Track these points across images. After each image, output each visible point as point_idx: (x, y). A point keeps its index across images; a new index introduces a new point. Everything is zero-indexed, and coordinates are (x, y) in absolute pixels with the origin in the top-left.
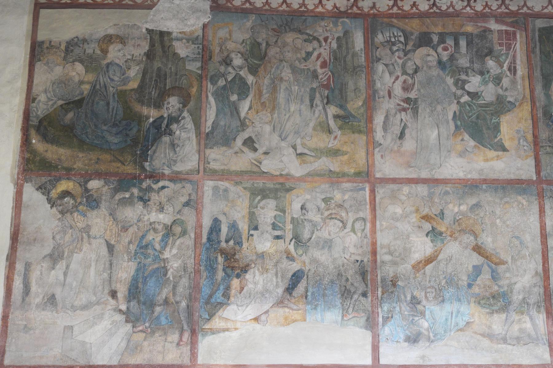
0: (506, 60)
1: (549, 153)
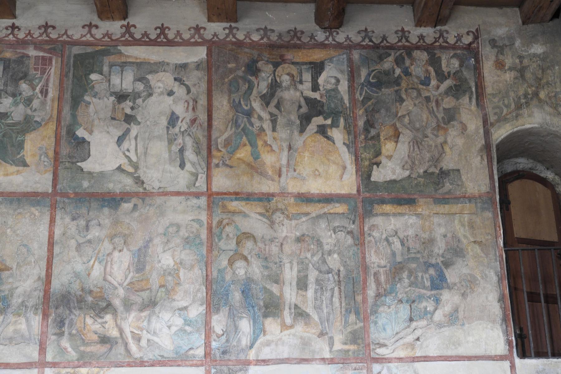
0: (39, 83)
1: (68, 168)
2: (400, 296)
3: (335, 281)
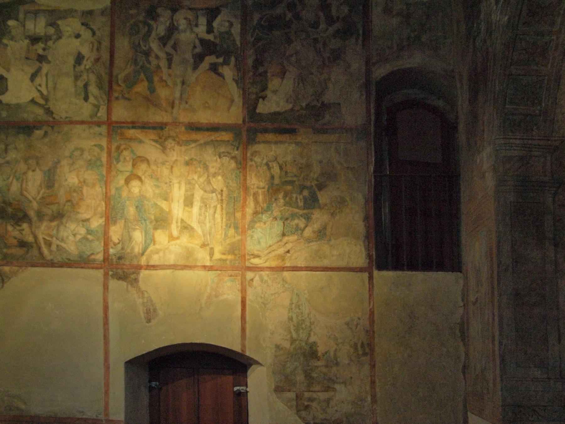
2: (275, 214)
3: (218, 200)
